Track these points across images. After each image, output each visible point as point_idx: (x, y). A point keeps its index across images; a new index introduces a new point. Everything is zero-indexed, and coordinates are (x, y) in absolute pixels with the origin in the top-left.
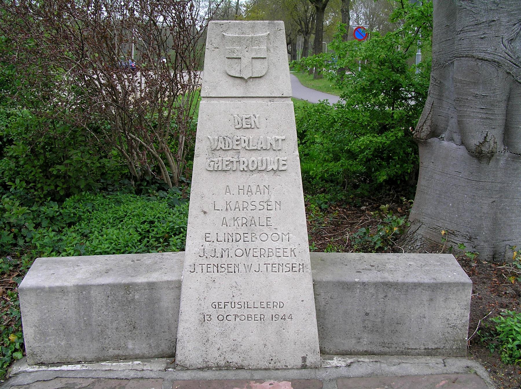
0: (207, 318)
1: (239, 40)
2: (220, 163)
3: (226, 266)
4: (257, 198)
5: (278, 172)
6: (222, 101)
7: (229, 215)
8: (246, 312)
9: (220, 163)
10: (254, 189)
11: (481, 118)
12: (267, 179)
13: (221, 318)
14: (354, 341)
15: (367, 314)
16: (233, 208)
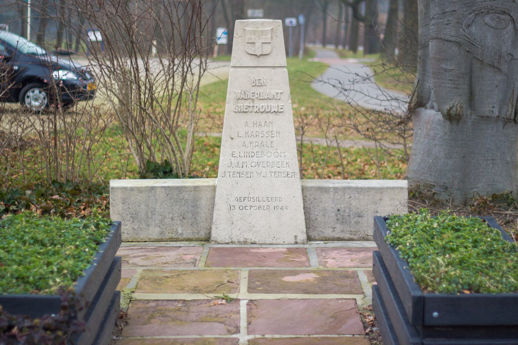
0: (232, 208)
1: (254, 32)
2: (242, 107)
3: (245, 173)
4: (265, 129)
5: (278, 113)
6: (244, 69)
7: (248, 140)
8: (257, 204)
9: (242, 107)
10: (263, 124)
11: (451, 88)
12: (271, 117)
13: (241, 208)
14: (331, 230)
15: (339, 210)
16: (250, 136)
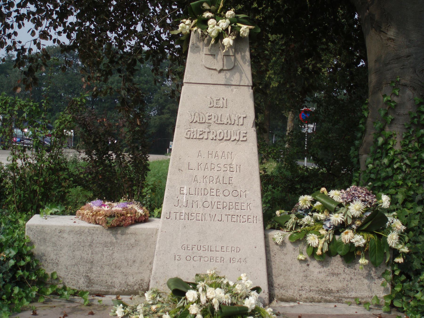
0: (177, 258)
2: (195, 133)
3: (195, 215)
4: (223, 161)
5: (240, 142)
7: (200, 174)
9: (195, 133)
10: (220, 154)
13: (188, 258)
16: (203, 169)
